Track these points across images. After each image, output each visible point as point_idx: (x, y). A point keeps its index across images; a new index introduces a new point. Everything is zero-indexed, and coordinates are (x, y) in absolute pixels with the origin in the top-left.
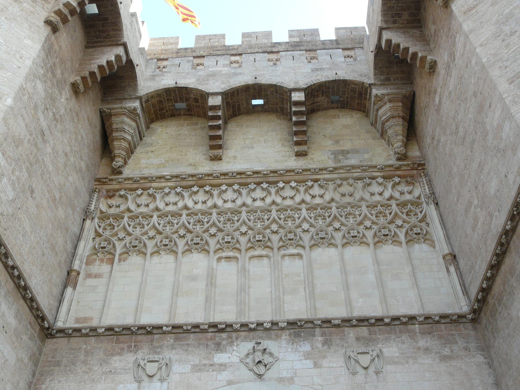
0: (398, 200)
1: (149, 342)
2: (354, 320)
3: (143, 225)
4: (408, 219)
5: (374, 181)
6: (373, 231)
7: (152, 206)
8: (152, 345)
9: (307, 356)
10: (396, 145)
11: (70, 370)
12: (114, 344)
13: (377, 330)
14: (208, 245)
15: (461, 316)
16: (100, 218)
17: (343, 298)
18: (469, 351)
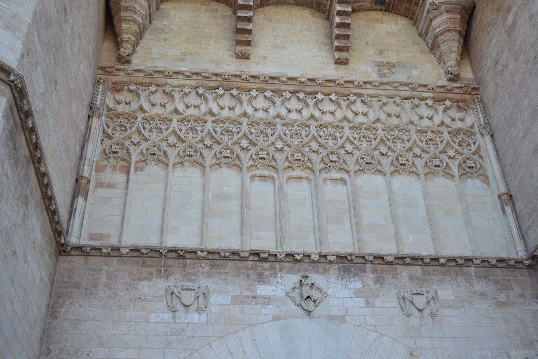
0: (450, 127)
1: (181, 267)
2: (408, 259)
3: (160, 129)
4: (461, 151)
5: (423, 103)
6: (424, 160)
7: (170, 107)
8: (185, 271)
9: (358, 293)
10: (448, 64)
11: (92, 294)
12: (140, 268)
13: (431, 271)
14: (240, 160)
15: (517, 262)
16: (106, 116)
17: (393, 232)
18: (525, 298)
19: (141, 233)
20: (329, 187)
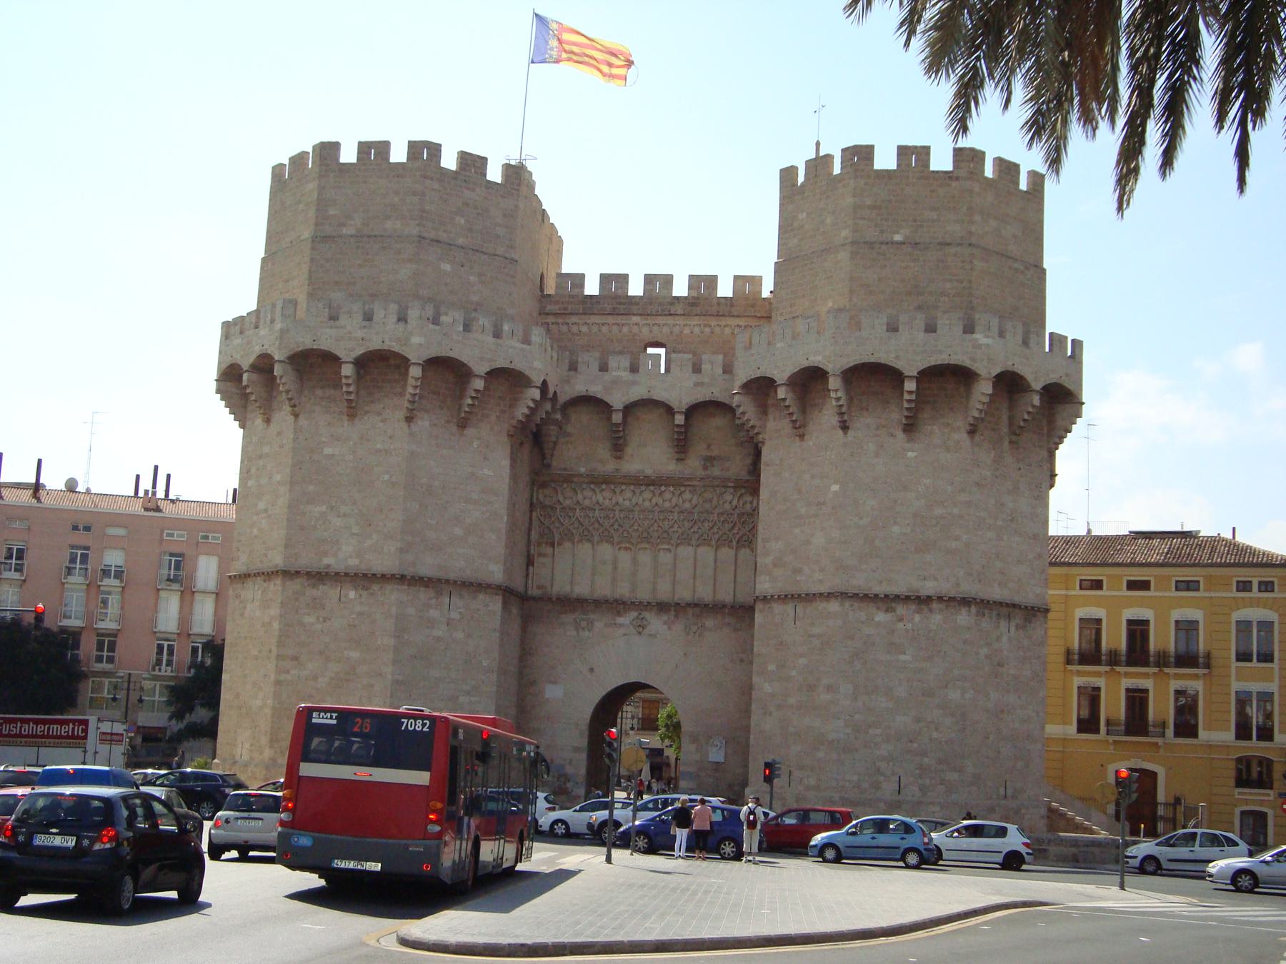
9: (665, 623)
19: (561, 585)
20: (662, 553)
